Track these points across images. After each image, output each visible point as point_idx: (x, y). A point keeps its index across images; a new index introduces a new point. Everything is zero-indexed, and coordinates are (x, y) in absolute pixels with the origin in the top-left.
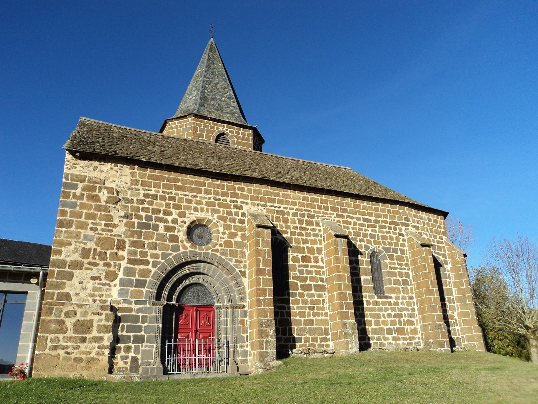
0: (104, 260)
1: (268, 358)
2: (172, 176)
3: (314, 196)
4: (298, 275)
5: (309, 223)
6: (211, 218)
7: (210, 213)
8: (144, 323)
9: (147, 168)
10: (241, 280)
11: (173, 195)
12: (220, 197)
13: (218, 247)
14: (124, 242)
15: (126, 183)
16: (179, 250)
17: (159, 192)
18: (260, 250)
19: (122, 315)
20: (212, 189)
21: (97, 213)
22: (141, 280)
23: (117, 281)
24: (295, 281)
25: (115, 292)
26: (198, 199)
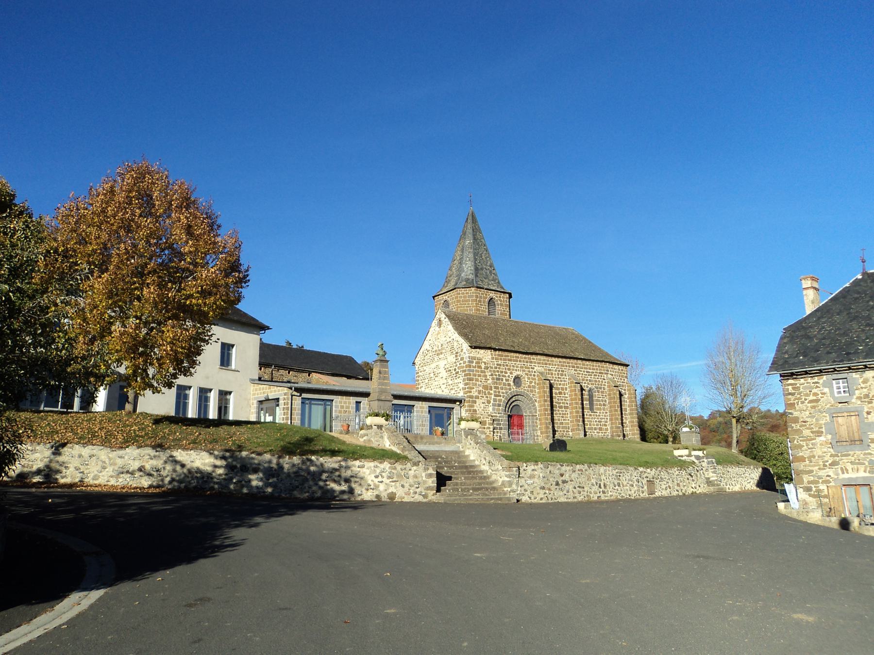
5: (562, 375)
25: (491, 409)
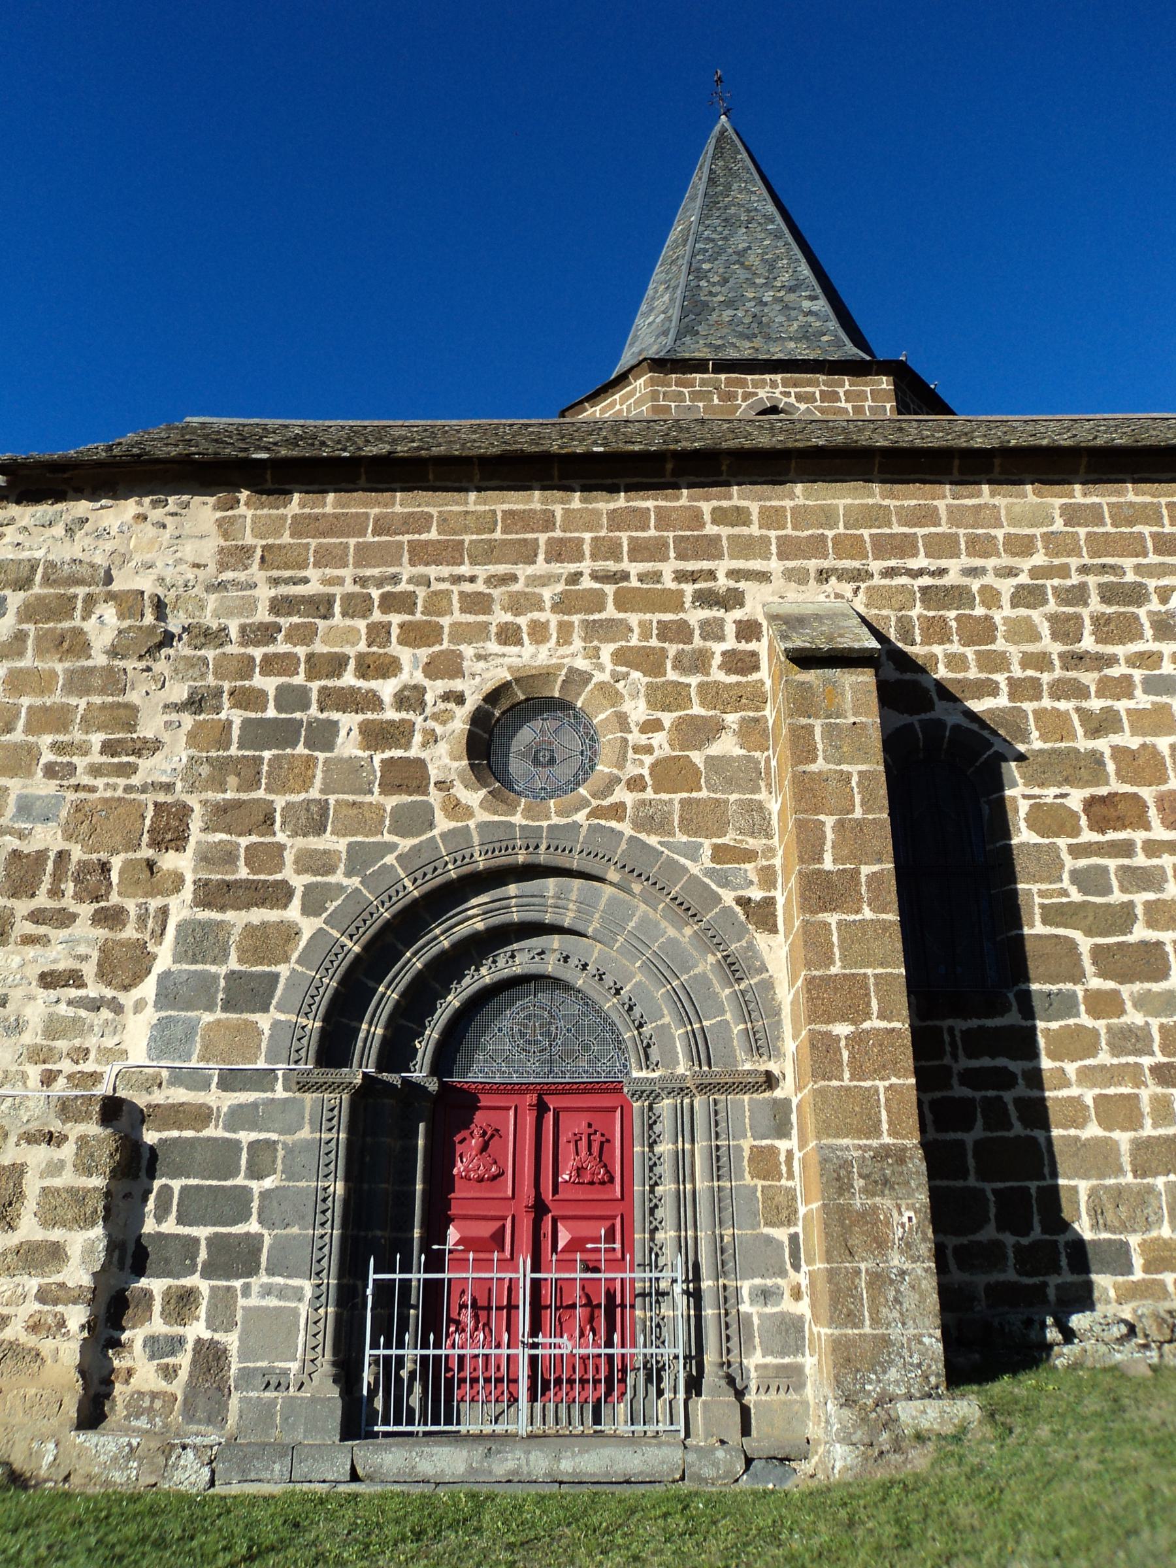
0: (97, 899)
1: (893, 1374)
2: (398, 509)
3: (1131, 497)
4: (1076, 896)
5: (1117, 629)
6: (582, 664)
7: (578, 644)
8: (260, 1177)
9: (290, 492)
10: (751, 946)
11: (403, 587)
12: (625, 565)
13: (621, 794)
14: (185, 811)
15: (198, 566)
16: (431, 826)
17: (340, 581)
18: (822, 778)
19: (163, 1141)
20: (587, 536)
21: (73, 701)
22: (252, 975)
23: (148, 988)
24: (1061, 931)
25: (136, 1035)
26: (517, 587)
